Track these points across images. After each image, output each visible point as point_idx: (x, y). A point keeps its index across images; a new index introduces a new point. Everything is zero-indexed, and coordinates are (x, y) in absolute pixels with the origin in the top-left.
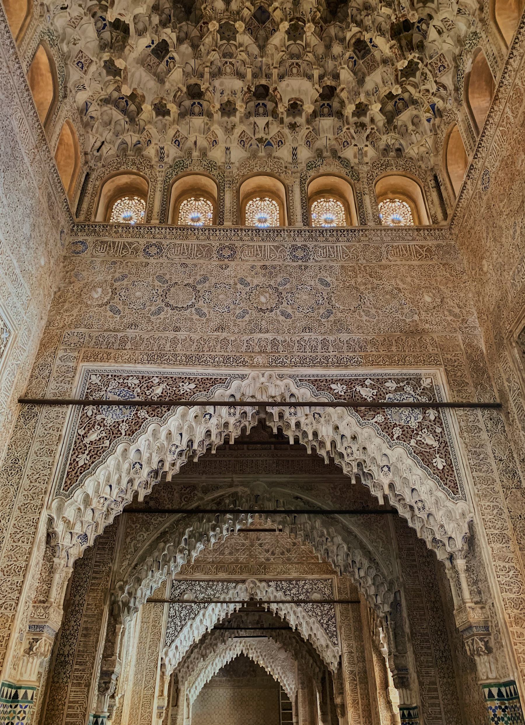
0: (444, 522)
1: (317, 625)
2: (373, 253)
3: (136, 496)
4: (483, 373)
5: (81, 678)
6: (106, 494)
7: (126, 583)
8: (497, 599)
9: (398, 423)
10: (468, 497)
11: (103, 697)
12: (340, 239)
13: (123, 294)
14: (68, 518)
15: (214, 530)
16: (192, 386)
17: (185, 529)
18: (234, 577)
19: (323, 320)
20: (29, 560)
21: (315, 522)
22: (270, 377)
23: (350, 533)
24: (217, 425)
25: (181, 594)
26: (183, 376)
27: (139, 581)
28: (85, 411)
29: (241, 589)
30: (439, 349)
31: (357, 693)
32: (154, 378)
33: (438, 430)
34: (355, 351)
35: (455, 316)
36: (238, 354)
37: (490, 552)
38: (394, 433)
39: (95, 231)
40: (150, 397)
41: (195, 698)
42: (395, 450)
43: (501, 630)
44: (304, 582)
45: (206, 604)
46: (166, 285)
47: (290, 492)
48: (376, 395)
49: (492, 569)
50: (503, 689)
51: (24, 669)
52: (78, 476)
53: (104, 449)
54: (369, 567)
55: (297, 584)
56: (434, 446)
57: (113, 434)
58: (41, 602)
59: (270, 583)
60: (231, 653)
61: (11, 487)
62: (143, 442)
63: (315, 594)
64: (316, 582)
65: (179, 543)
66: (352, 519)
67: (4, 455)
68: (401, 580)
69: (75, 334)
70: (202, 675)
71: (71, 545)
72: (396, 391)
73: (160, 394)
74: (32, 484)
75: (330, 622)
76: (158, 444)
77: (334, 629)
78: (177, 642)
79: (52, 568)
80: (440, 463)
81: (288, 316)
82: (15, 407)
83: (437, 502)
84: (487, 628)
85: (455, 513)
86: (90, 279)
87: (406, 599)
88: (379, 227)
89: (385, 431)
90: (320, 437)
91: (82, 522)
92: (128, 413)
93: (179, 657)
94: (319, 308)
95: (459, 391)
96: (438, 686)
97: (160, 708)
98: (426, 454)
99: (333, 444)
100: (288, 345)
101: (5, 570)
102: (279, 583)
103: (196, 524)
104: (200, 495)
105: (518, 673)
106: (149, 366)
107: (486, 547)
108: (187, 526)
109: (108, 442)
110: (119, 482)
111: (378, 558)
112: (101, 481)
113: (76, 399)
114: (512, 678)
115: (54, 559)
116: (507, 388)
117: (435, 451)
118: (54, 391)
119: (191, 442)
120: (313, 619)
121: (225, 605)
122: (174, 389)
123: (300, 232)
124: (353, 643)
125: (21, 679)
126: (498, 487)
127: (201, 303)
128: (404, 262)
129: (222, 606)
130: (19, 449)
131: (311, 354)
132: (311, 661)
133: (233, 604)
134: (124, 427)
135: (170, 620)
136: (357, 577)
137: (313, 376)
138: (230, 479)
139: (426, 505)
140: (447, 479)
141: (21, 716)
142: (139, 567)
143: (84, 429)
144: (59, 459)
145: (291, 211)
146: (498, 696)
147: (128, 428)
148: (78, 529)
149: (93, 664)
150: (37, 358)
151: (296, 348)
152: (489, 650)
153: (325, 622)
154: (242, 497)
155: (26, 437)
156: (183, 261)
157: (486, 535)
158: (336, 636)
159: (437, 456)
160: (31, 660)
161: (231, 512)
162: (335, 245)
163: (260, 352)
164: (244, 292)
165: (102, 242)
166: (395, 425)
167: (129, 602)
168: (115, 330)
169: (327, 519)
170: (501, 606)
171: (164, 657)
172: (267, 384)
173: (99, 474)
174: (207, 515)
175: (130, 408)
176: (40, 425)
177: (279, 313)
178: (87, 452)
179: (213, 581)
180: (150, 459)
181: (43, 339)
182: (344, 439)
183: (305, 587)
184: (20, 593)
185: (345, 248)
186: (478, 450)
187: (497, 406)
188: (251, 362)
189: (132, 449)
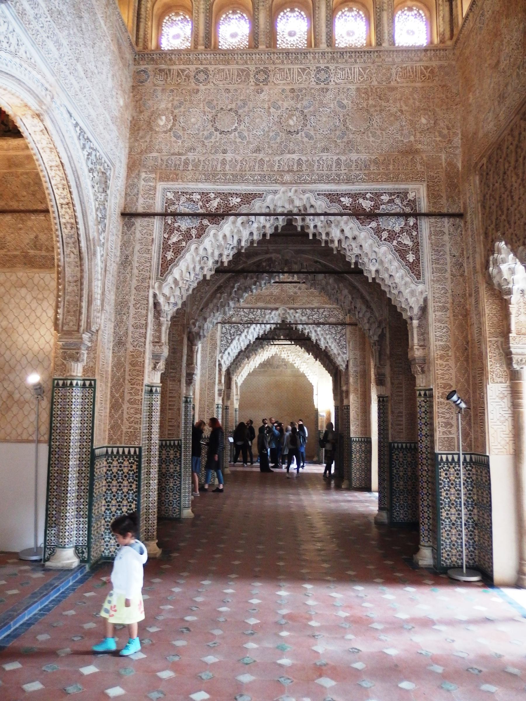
2: (384, 74)
3: (205, 276)
4: (456, 188)
5: (175, 377)
7: (197, 320)
10: (426, 281)
12: (358, 61)
13: (181, 120)
15: (255, 284)
16: (239, 200)
17: (234, 284)
18: (269, 306)
19: (338, 141)
22: (296, 191)
23: (354, 287)
24: (257, 228)
27: (205, 319)
29: (275, 314)
33: (414, 233)
34: (361, 170)
35: (444, 136)
39: (153, 59)
41: (241, 382)
46: (214, 111)
50: (427, 392)
58: (157, 342)
65: (231, 294)
66: (357, 278)
72: (388, 202)
78: (229, 350)
80: (411, 258)
81: (311, 138)
82: (119, 219)
83: (405, 284)
84: (424, 360)
86: (155, 108)
88: (392, 48)
90: (330, 236)
91: (174, 296)
92: (196, 223)
93: (231, 359)
94: (336, 130)
95: (435, 203)
97: (220, 390)
99: (340, 241)
100: (310, 165)
103: (242, 281)
104: (244, 259)
106: (206, 184)
108: (236, 281)
110: (194, 269)
111: (373, 306)
119: (239, 241)
120: (328, 336)
121: (263, 326)
123: (323, 53)
124: (358, 353)
126: (448, 275)
127: (242, 127)
128: (409, 84)
131: (327, 172)
136: (357, 317)
137: (328, 191)
141: (156, 400)
142: (204, 310)
144: (155, 256)
145: (317, 16)
148: (172, 300)
151: (316, 167)
154: (275, 261)
156: (227, 86)
158: (346, 347)
159: (410, 252)
161: (267, 272)
162: (353, 67)
163: (289, 171)
164: (276, 116)
165: (160, 70)
166: (384, 230)
168: (180, 154)
174: (250, 274)
177: (304, 135)
178: (171, 250)
179: (253, 308)
180: (213, 253)
184: (145, 338)
185: (361, 69)
186: (439, 249)
187: (460, 216)
189: (201, 248)
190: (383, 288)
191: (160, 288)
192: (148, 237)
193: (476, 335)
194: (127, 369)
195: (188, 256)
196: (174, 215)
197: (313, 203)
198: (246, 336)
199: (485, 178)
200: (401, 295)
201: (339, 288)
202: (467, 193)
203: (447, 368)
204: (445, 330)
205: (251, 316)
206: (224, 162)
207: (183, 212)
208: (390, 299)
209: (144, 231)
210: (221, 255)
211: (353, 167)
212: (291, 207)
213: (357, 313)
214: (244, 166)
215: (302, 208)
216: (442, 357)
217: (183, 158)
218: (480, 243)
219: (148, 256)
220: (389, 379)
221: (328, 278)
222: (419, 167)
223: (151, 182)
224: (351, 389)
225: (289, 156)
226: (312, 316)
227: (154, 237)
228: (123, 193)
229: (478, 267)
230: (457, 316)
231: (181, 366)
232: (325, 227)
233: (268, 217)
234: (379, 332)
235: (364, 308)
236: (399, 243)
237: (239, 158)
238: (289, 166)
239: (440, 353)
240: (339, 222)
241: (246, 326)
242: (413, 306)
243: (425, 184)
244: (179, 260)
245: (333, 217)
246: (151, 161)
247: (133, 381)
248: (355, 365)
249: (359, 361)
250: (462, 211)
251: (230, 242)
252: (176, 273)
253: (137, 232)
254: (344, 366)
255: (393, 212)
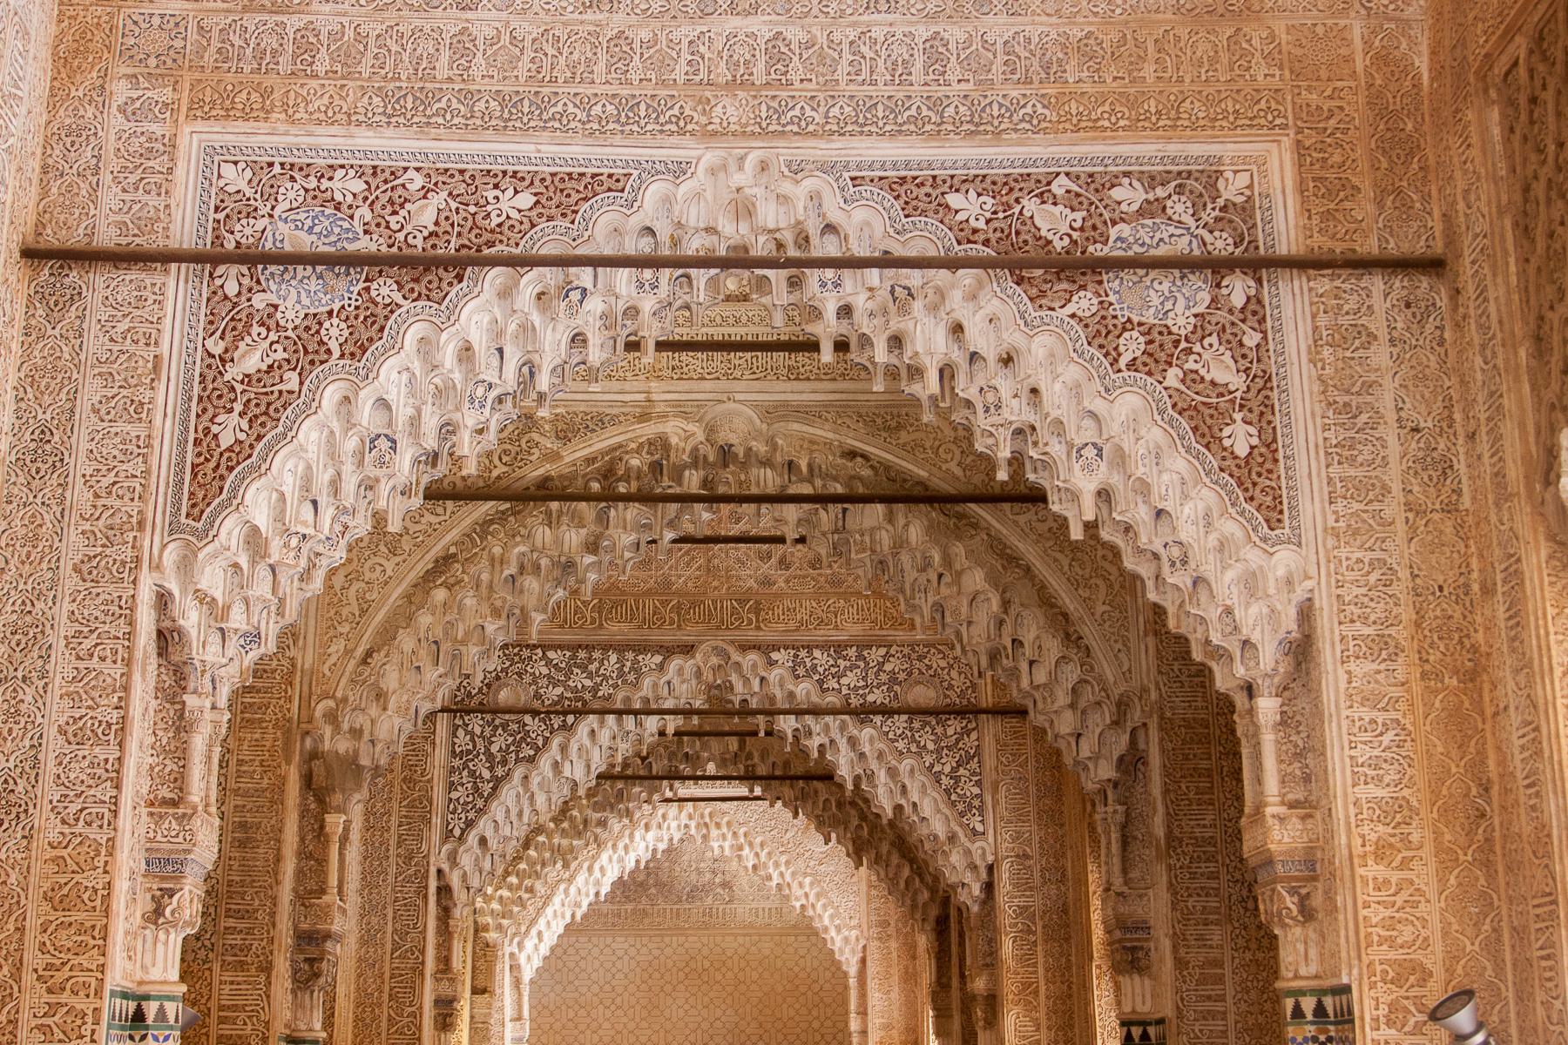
0: (1235, 601)
1: (921, 778)
3: (379, 519)
4: (1411, 154)
6: (305, 523)
8: (1339, 801)
9: (1136, 319)
10: (1307, 536)
11: (307, 997)
14: (210, 592)
16: (525, 200)
18: (656, 636)
20: (127, 706)
21: (907, 525)
22: (764, 166)
23: (1011, 559)
24: (604, 316)
25: (489, 686)
26: (496, 168)
28: (218, 282)
29: (680, 671)
30: (1287, 72)
31: (1035, 965)
32: (411, 174)
33: (1252, 339)
36: (663, 93)
37: (1343, 685)
38: (1122, 349)
40: (401, 236)
41: (537, 962)
42: (1120, 400)
43: (1338, 873)
44: (882, 651)
45: (570, 719)
47: (830, 435)
48: (1082, 229)
49: (1340, 728)
50: (1328, 1002)
51: (148, 958)
52: (222, 478)
53: (287, 399)
54: (1064, 658)
55: (860, 657)
56: (1232, 388)
57: (306, 352)
58: (166, 802)
59: (775, 656)
60: (650, 836)
61: (43, 510)
62: (394, 375)
63: (919, 689)
64: (922, 650)
66: (1022, 519)
67: (7, 419)
68: (1154, 695)
69: (156, 21)
70: (557, 900)
71: (224, 661)
72: (1141, 213)
73: (432, 228)
74: (100, 503)
75: (962, 771)
76: (436, 380)
77: (976, 791)
78: (484, 826)
79: (181, 717)
80: (1240, 437)
83: (1221, 547)
84: (1310, 863)
85: (1265, 577)
87: (1163, 750)
89: (1097, 342)
90: (908, 353)
92: (344, 290)
95: (1327, 215)
96: (1228, 971)
98: (1207, 412)
101: (70, 730)
102: (803, 653)
104: (549, 444)
105: (1360, 969)
106: (390, 132)
107: (1335, 671)
109: (294, 376)
110: (335, 486)
111: (1090, 633)
112: (287, 490)
113: (185, 246)
114: (1345, 980)
115: (185, 697)
116: (1462, 219)
117: (1233, 401)
118: (118, 218)
119: (530, 371)
120: (907, 763)
121: (629, 721)
122: (472, 209)
124: (1032, 831)
125: (146, 978)
126: (1393, 508)
129: (620, 722)
130: (47, 399)
132: (906, 872)
133: (657, 717)
134: (334, 332)
135: (457, 763)
136: (1025, 683)
138: (642, 397)
139: (1190, 554)
140: (1255, 484)
143: (222, 338)
146: (1315, 1015)
147: (346, 333)
149: (273, 914)
150: (52, 108)
151: (843, 68)
152: (1307, 913)
153: (947, 769)
155: (60, 364)
157: (1337, 639)
158: (981, 810)
159: (1238, 416)
160: (162, 936)
163: (733, 85)
167: (356, 753)
169: (942, 518)
170: (1347, 817)
171: (445, 867)
172: (755, 190)
173: (280, 471)
175: (348, 274)
176: (95, 327)
178: (238, 407)
179: (589, 648)
180: (415, 422)
181: (59, 39)
182: (978, 365)
183: (888, 667)
184: (118, 787)
187: (1433, 265)
188: (704, 120)
189: (366, 398)
190: (1129, 563)
191: (186, 565)
192: (140, 350)
193: (1518, 757)
194: (32, 922)
195: (310, 434)
196: (253, 258)
197: (835, 216)
198: (556, 766)
199: (1524, 117)
200: (1203, 596)
201: (948, 561)
202: (1458, 174)
203: (1404, 896)
204: (1390, 736)
205: (580, 680)
206: (463, 46)
207: (288, 248)
208: (1159, 611)
209: (123, 326)
210: (448, 429)
211: (998, 67)
212: (744, 228)
213: (1024, 666)
214: (546, 63)
215: (788, 237)
216: (1381, 852)
217: (294, 22)
218: (1517, 379)
219: (134, 430)
220: (1166, 944)
221: (901, 521)
222: (1260, 70)
223: (155, 120)
224: (1009, 987)
225: (734, 23)
226: (838, 676)
227: (164, 348)
228: (35, 164)
229: (1514, 473)
230: (1439, 677)
231: (275, 901)
232: (885, 312)
233: (648, 274)
234: (1120, 743)
235: (1053, 648)
236: (1191, 378)
237: (527, 29)
238: (733, 64)
239: (1375, 832)
240: (941, 294)
241: (556, 721)
242: (1255, 637)
243: (1287, 142)
244: (270, 447)
245: (917, 273)
246: (156, 34)
247: (60, 976)
248: (1023, 885)
249: (1036, 865)
250: (1439, 248)
251: (490, 376)
252: (257, 503)
253: (92, 328)
254: (976, 890)
255: (1162, 251)
